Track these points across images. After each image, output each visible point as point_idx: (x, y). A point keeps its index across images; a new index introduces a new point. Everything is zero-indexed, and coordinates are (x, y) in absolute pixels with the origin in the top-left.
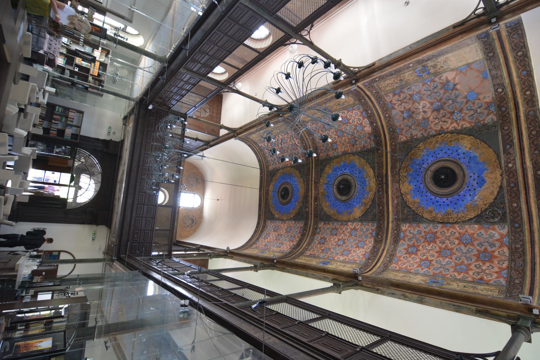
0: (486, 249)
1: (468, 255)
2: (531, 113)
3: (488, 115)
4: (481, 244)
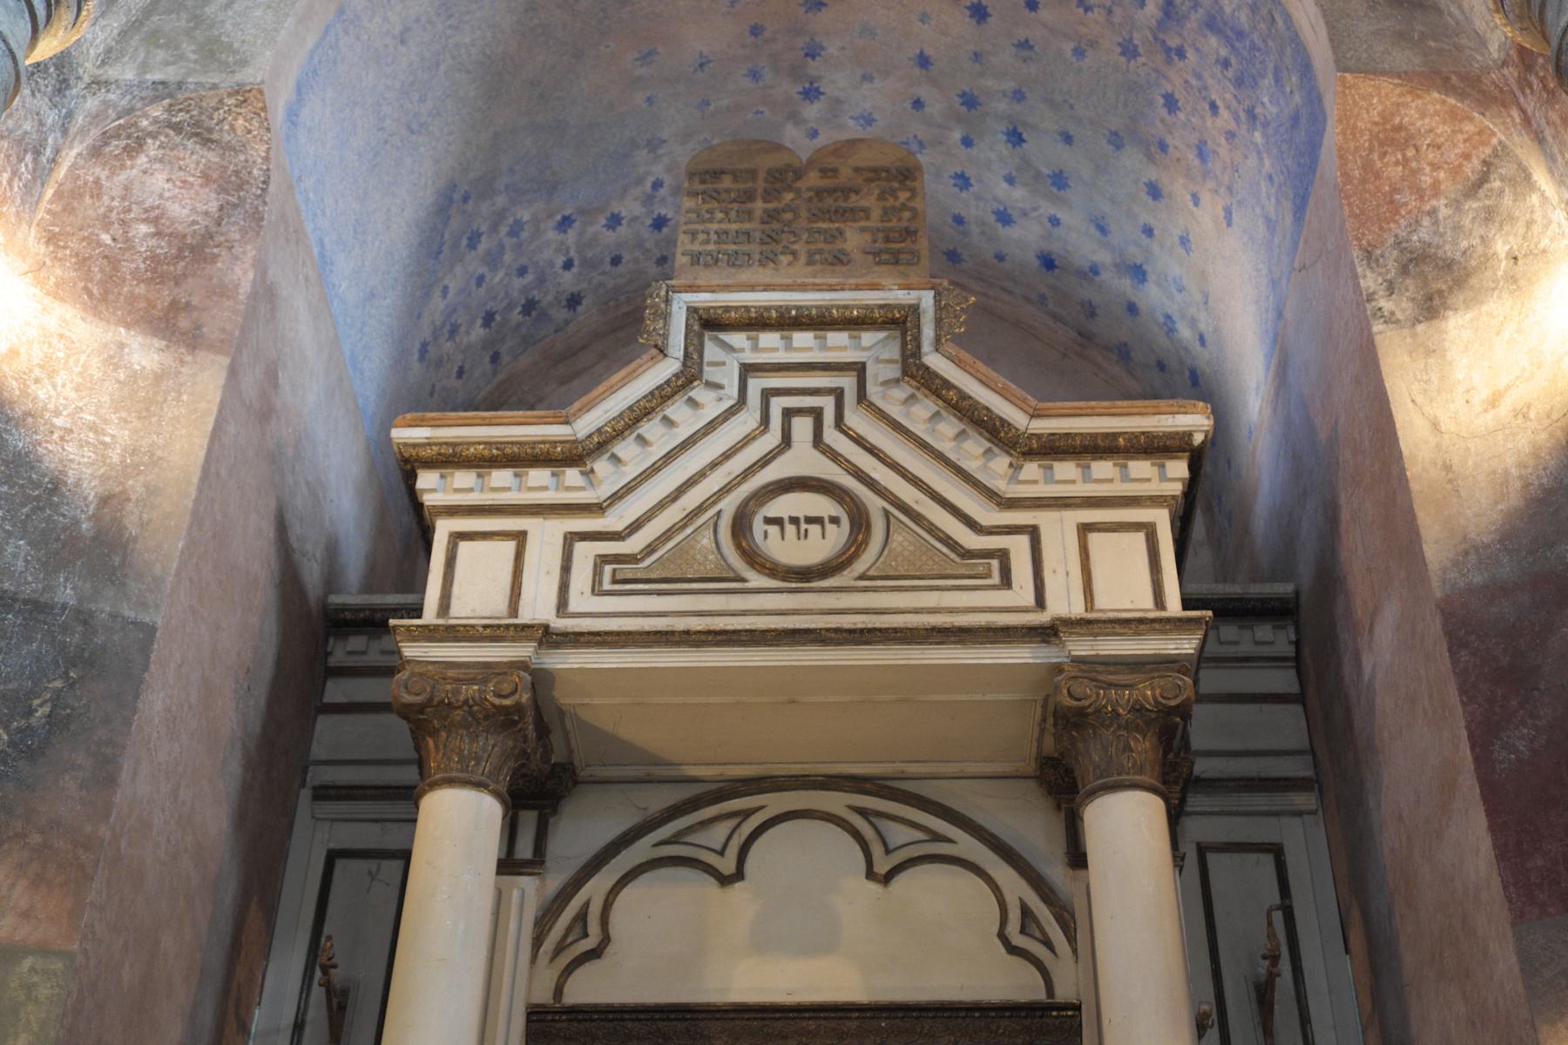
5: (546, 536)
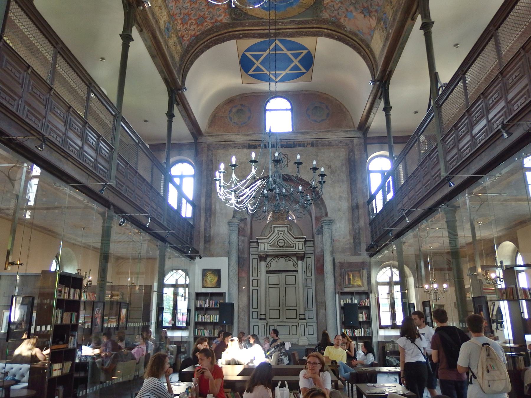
0: (207, 17)
1: (198, 12)
2: (321, 34)
3: (330, 15)
4: (210, 13)
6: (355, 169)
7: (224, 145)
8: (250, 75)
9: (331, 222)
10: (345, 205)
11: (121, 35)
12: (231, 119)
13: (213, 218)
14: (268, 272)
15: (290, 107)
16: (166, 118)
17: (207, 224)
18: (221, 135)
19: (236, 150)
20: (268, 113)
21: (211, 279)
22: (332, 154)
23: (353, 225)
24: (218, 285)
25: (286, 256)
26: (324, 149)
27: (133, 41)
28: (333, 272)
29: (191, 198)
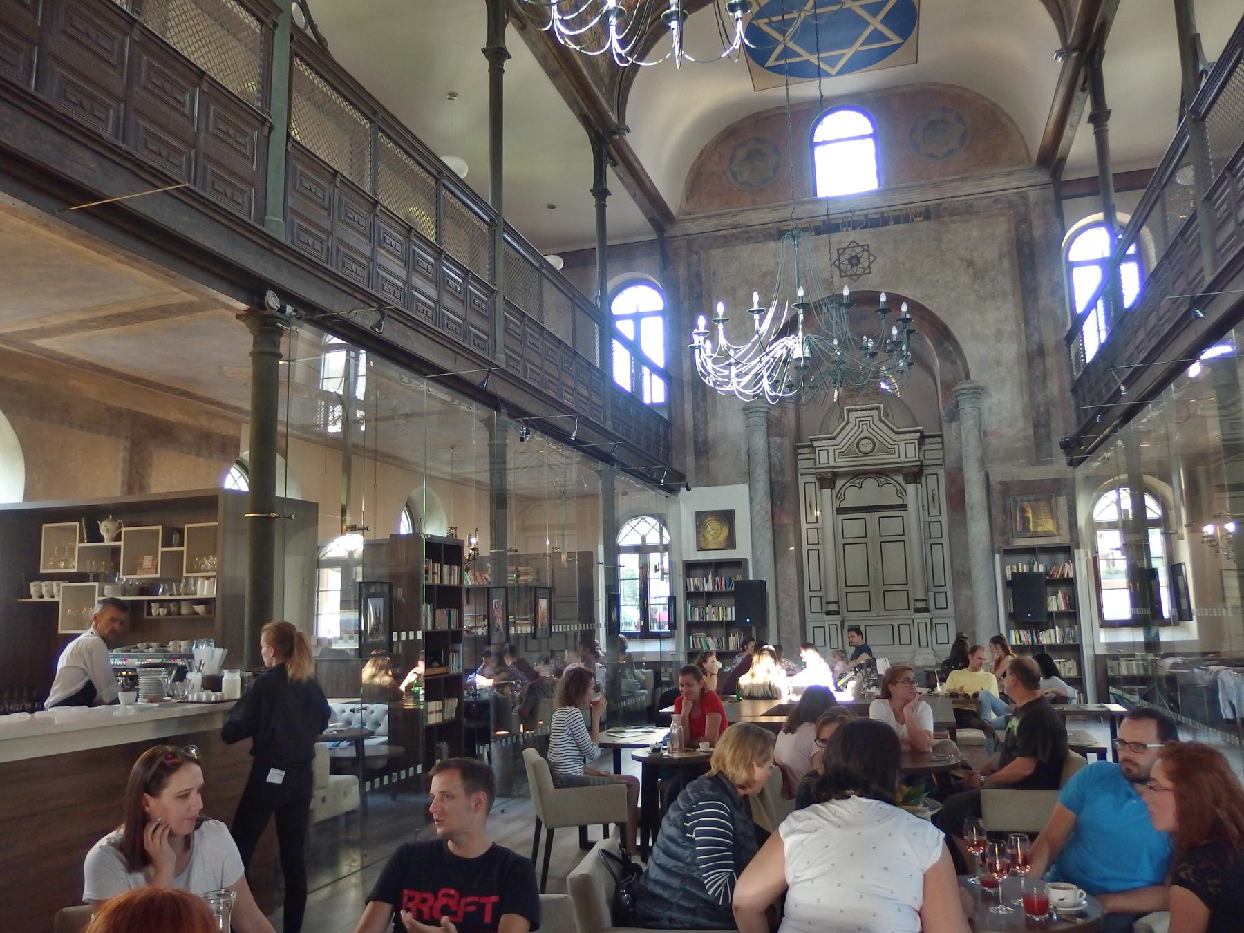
5: (831, 449)
6: (1033, 261)
7: (724, 237)
8: (771, 69)
9: (978, 391)
10: (1010, 351)
11: (484, 51)
12: (734, 175)
13: (710, 401)
14: (840, 511)
15: (870, 130)
16: (592, 200)
17: (699, 416)
18: (714, 216)
19: (751, 246)
20: (819, 152)
21: (715, 531)
22: (976, 233)
23: (1032, 394)
24: (731, 543)
25: (880, 473)
26: (955, 222)
27: (510, 57)
28: (985, 504)
29: (661, 363)
